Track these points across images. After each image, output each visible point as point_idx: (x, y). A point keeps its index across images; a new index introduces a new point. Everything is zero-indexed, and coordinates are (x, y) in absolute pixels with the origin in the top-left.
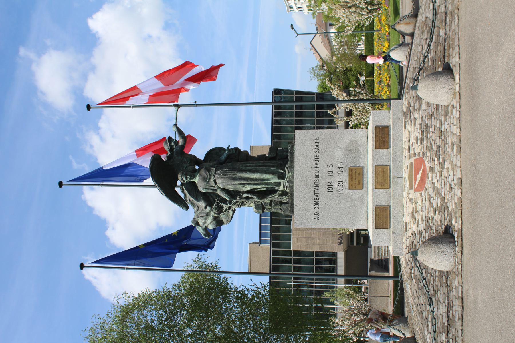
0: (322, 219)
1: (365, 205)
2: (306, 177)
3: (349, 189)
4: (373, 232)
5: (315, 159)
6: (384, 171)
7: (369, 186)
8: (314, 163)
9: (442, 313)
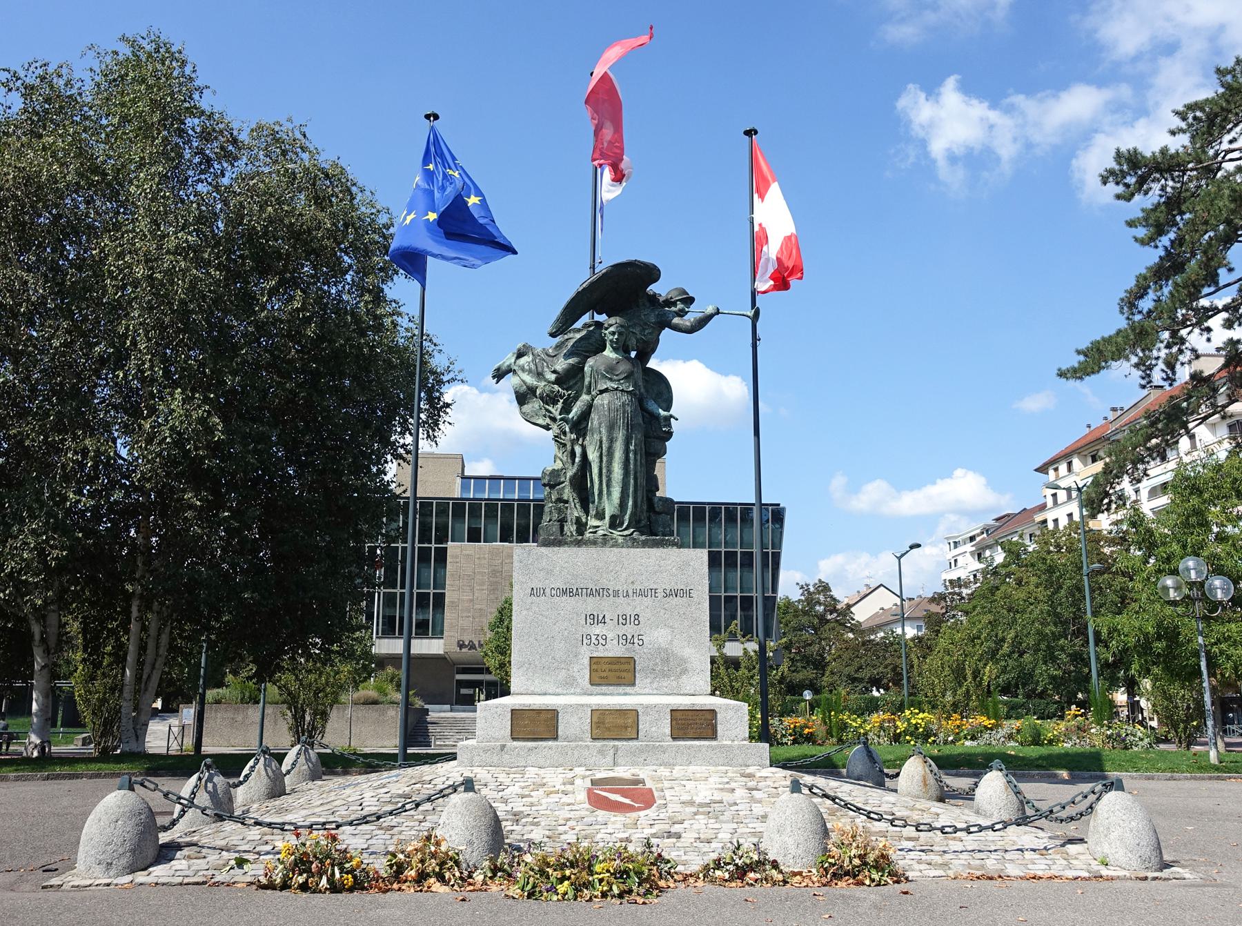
1: (559, 690)
4: (504, 706)
6: (626, 728)
9: (346, 842)
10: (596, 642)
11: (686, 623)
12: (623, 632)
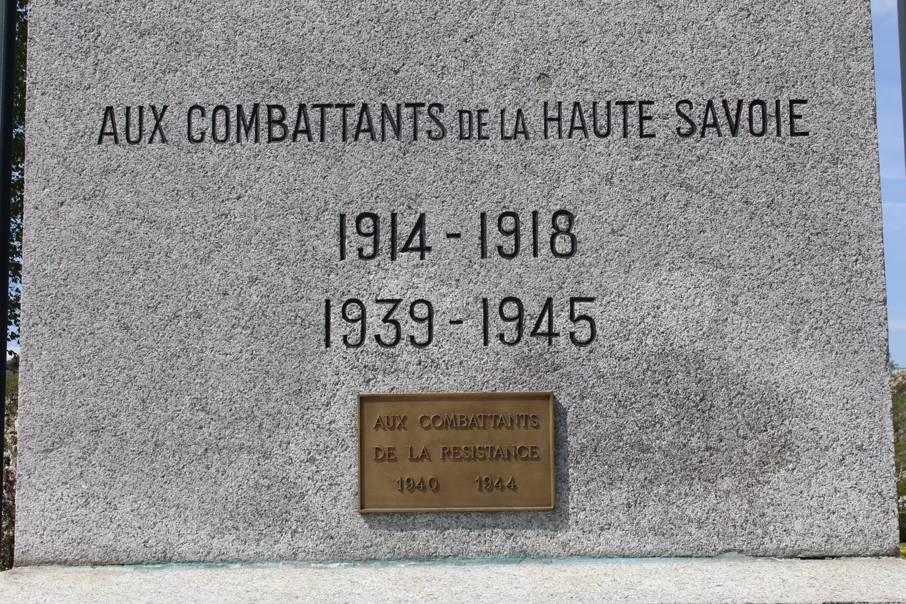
0: (106, 172)
1: (227, 544)
2: (462, 33)
3: (363, 399)
5: (624, 104)
7: (392, 571)
8: (589, 97)
10: (388, 334)
11: (781, 244)
12: (506, 287)
